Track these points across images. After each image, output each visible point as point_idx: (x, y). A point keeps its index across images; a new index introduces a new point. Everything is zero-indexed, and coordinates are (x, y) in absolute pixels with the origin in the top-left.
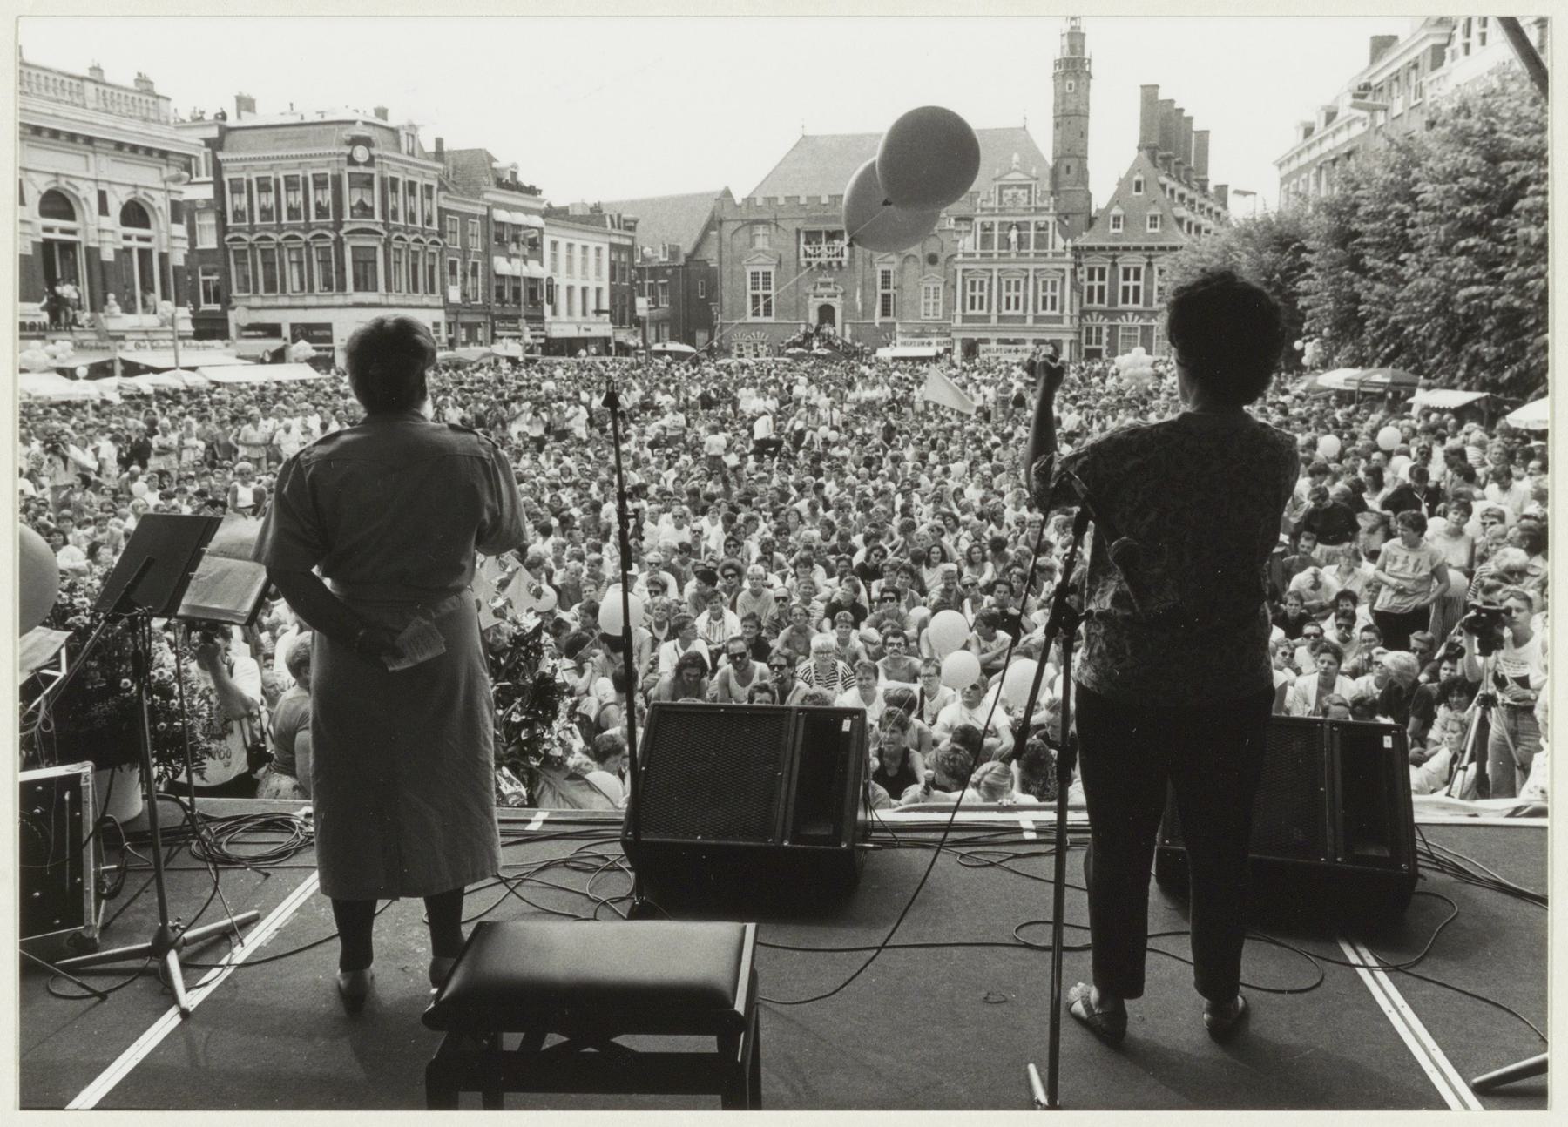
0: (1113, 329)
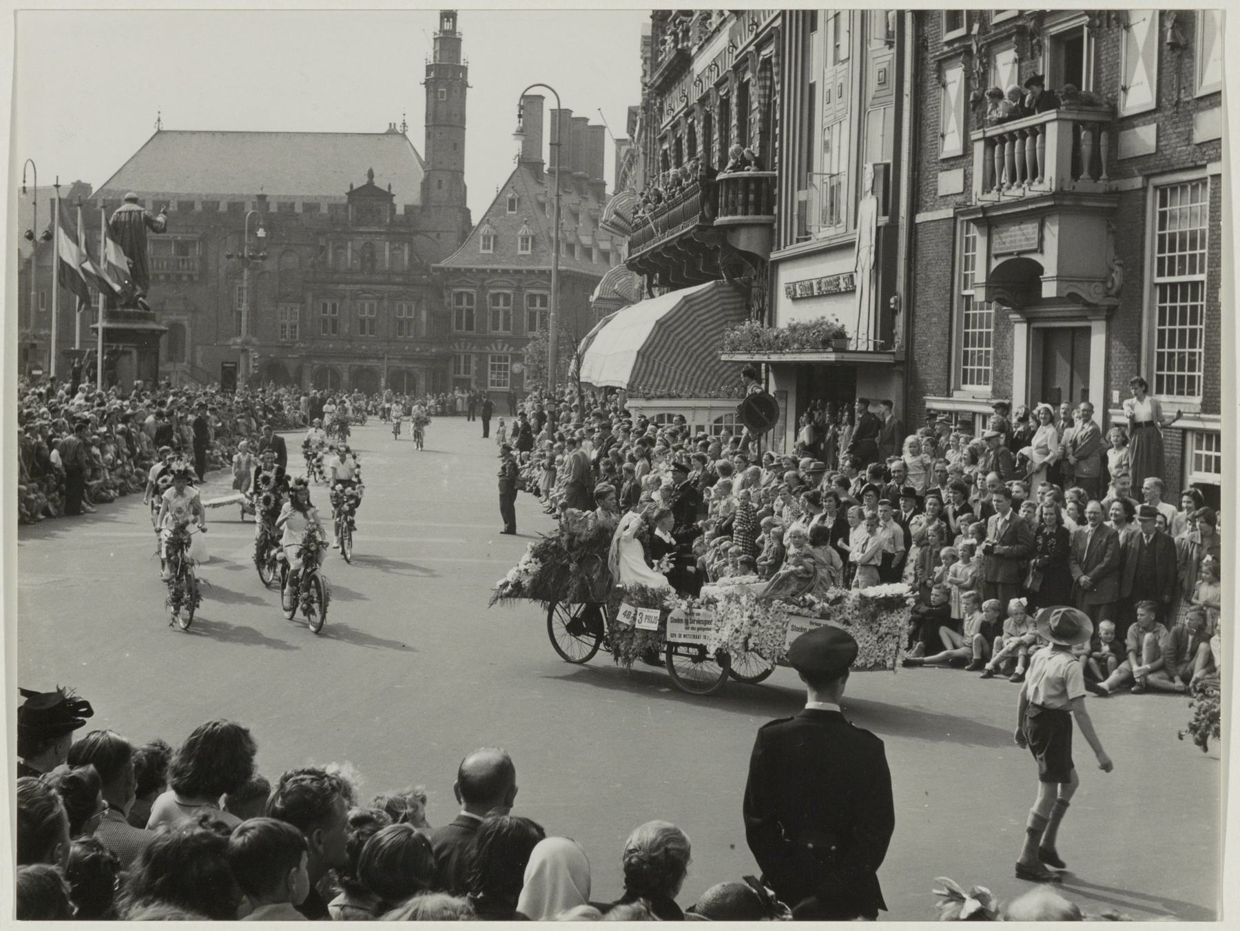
0: (482, 358)
